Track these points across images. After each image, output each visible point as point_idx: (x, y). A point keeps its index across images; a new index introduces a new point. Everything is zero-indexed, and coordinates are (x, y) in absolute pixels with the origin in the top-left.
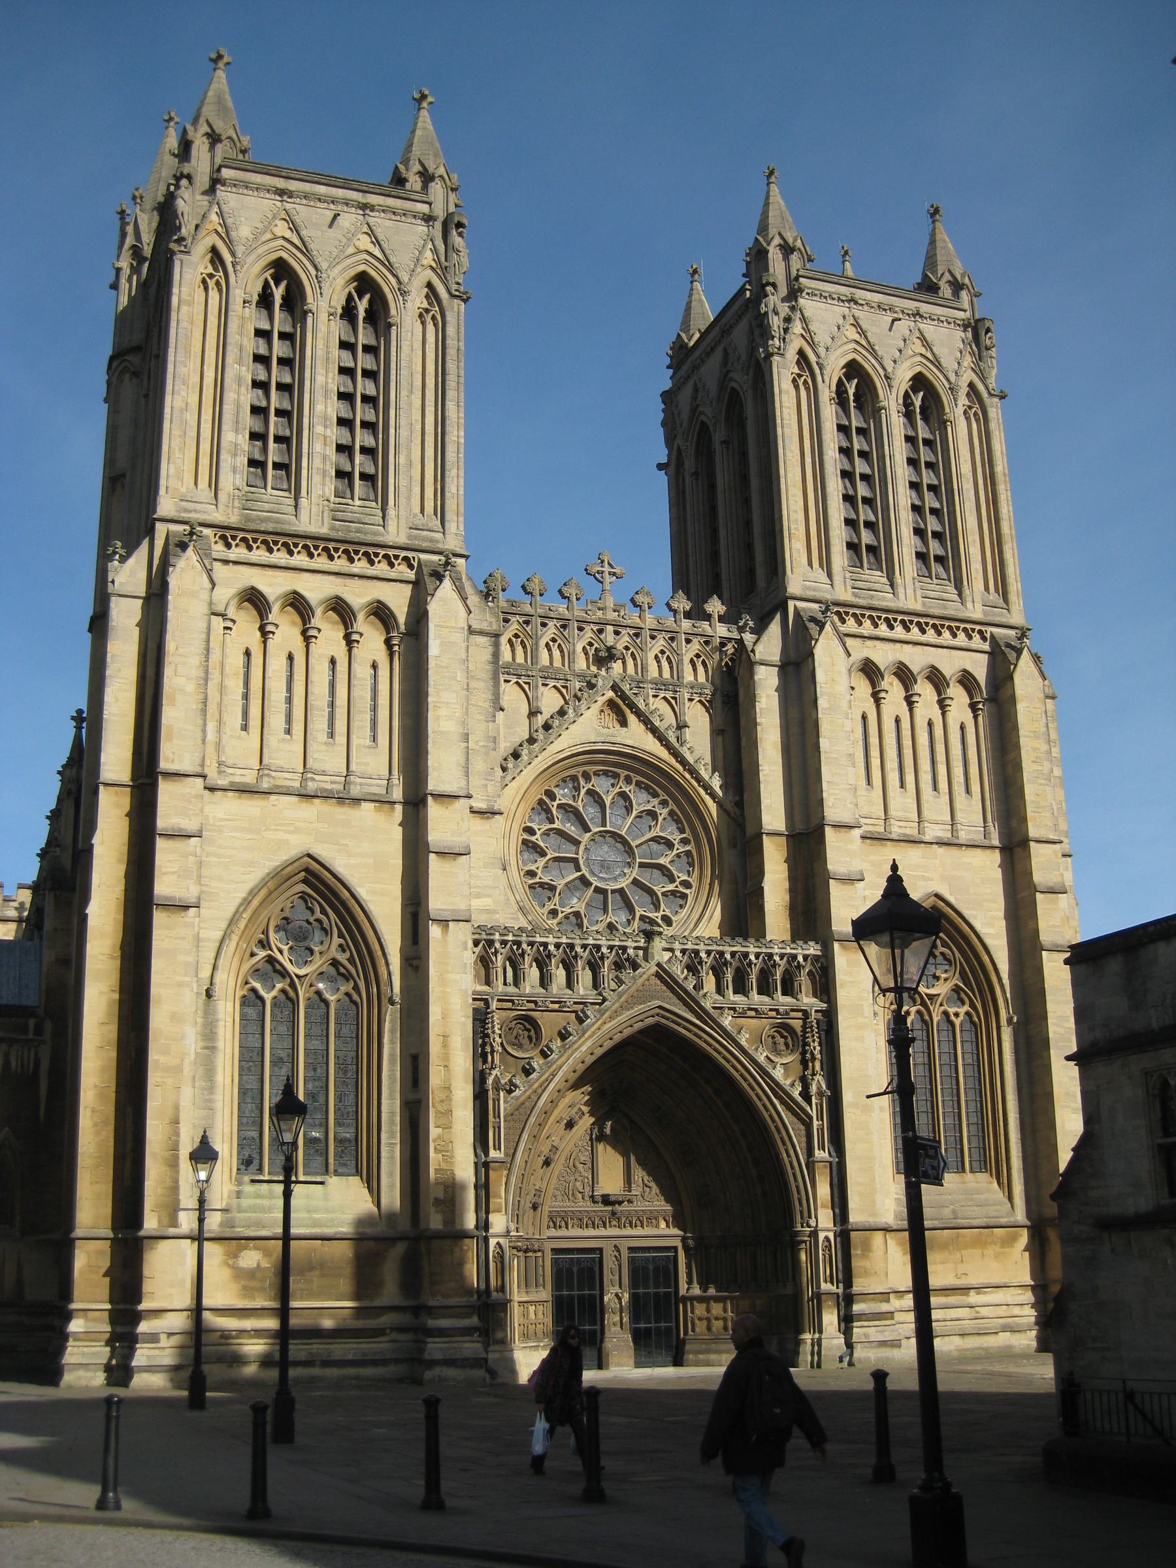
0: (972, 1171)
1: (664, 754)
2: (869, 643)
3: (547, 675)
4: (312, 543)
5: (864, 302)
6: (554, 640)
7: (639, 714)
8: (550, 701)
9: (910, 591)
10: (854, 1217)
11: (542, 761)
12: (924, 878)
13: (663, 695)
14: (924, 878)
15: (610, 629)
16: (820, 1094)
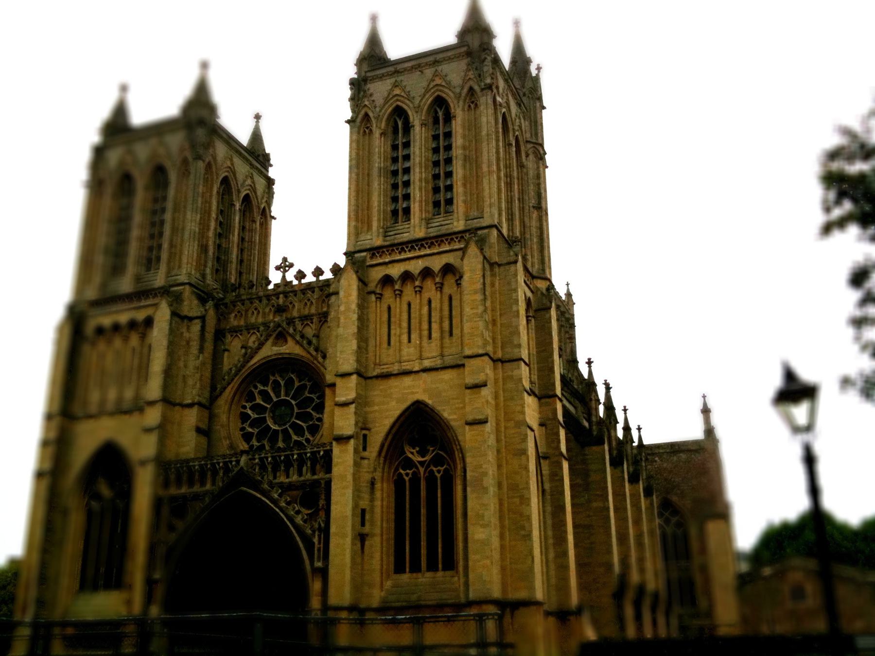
0: (410, 572)
1: (304, 354)
2: (390, 266)
3: (250, 328)
4: (128, 297)
5: (403, 70)
6: (256, 309)
7: (291, 335)
8: (252, 341)
9: (417, 229)
10: (333, 600)
11: (245, 372)
12: (413, 393)
13: (305, 323)
14: (413, 393)
15: (281, 296)
16: (320, 529)
